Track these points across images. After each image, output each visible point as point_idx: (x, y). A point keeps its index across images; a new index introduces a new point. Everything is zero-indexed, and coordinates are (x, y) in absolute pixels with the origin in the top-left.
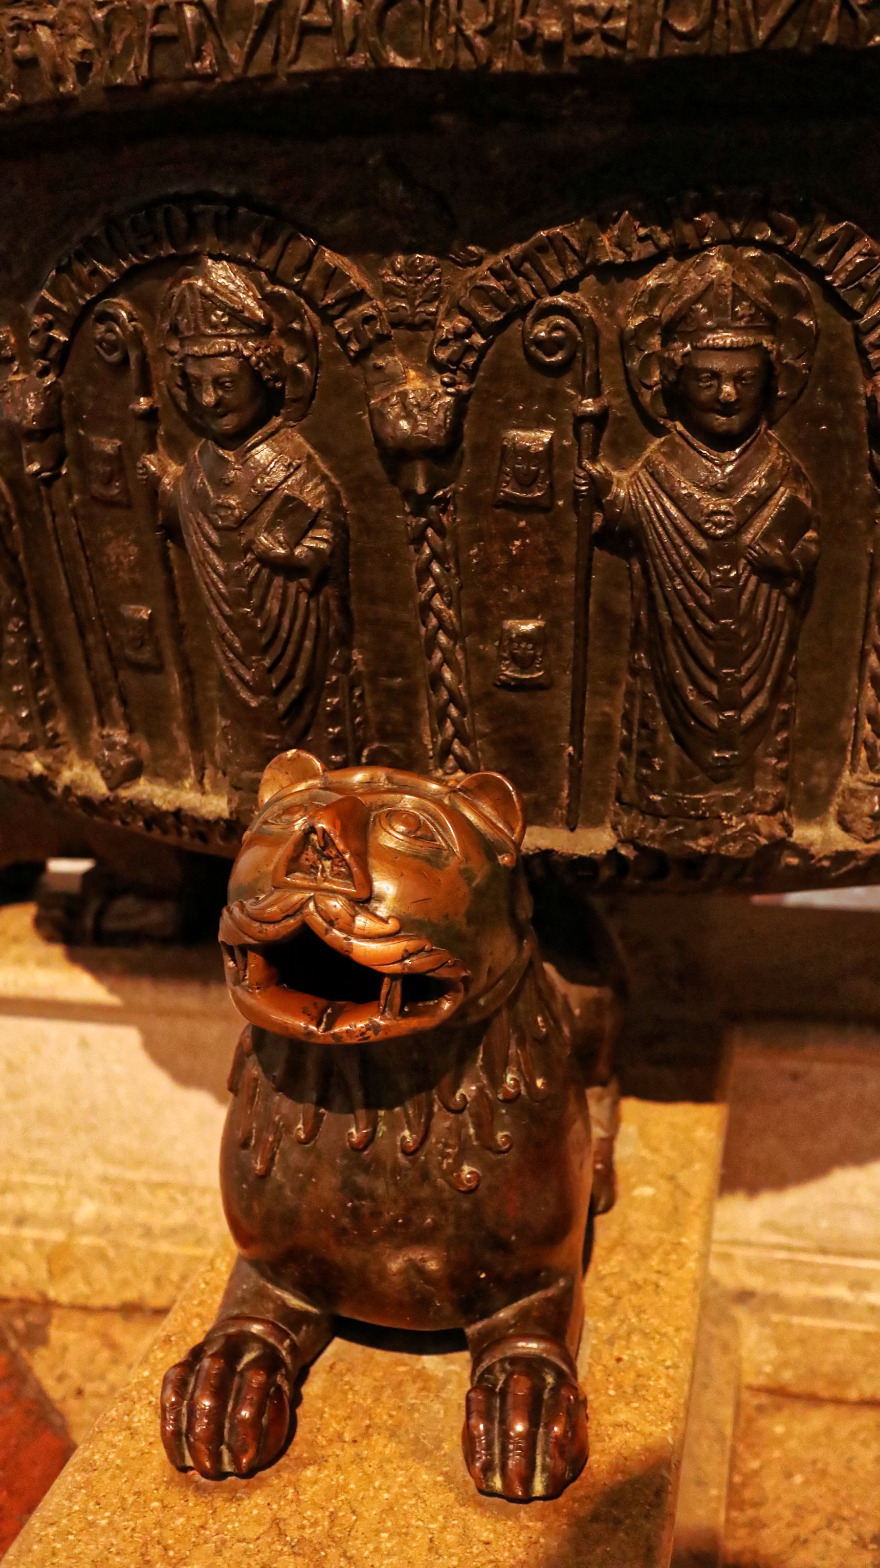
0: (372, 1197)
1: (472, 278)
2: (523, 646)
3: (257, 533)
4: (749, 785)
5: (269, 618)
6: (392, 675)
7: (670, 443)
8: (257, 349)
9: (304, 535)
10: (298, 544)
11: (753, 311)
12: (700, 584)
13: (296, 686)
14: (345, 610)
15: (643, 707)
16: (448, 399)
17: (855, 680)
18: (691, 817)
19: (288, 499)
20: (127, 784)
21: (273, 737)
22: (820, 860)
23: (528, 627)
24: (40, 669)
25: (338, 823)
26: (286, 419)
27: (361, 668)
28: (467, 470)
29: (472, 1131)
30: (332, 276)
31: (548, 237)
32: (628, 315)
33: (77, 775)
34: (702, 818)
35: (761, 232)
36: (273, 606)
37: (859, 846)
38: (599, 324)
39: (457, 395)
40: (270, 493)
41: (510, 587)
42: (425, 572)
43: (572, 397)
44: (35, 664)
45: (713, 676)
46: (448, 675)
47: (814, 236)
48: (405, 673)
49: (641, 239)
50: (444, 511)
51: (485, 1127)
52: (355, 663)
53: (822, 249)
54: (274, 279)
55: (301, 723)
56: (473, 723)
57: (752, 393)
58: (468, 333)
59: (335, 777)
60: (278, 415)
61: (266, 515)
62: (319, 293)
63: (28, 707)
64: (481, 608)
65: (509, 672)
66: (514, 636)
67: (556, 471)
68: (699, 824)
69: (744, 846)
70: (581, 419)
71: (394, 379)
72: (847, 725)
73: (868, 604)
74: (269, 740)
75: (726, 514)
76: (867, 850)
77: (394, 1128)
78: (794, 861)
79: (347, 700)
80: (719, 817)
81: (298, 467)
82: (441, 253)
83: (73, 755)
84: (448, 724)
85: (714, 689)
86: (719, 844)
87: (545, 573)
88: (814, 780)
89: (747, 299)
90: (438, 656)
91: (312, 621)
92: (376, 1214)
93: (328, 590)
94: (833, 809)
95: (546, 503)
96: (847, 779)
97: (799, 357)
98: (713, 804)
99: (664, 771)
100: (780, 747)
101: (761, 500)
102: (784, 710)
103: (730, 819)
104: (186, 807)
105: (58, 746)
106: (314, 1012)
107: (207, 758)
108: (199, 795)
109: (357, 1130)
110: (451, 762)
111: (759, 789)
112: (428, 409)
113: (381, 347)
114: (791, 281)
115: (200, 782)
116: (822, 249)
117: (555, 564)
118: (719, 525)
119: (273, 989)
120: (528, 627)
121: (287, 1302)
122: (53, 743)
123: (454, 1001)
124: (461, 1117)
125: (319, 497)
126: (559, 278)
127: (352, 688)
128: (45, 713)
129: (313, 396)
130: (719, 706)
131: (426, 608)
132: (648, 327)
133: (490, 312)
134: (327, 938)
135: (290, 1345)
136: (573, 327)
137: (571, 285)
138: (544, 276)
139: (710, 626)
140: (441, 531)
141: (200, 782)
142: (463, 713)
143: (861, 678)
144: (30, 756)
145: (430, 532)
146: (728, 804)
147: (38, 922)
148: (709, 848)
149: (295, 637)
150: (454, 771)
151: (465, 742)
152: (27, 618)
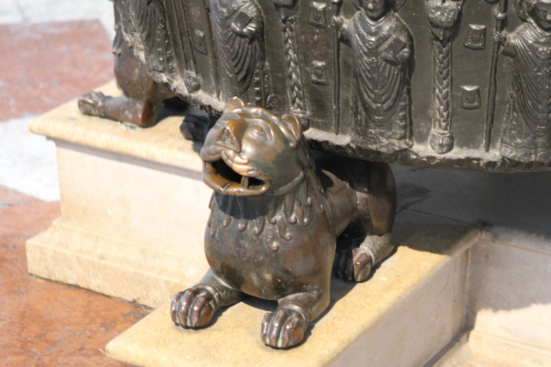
0: (244, 248)
3: (231, 22)
4: (390, 129)
5: (235, 49)
6: (278, 72)
7: (361, 14)
9: (247, 24)
10: (245, 27)
12: (366, 62)
13: (243, 73)
17: (433, 96)
18: (369, 137)
19: (242, 13)
20: (195, 92)
21: (237, 88)
22: (423, 158)
23: (320, 64)
24: (168, 44)
25: (233, 128)
27: (268, 68)
28: (300, 12)
29: (278, 231)
33: (179, 84)
36: (237, 46)
37: (437, 155)
40: (236, 11)
41: (314, 50)
42: (286, 41)
44: (167, 41)
45: (372, 92)
46: (294, 76)
50: (292, 23)
51: (283, 230)
52: (266, 66)
55: (245, 85)
57: (379, 7)
59: (246, 109)
61: (235, 16)
63: (163, 57)
64: (305, 56)
65: (314, 78)
66: (315, 67)
67: (327, 16)
68: (373, 140)
72: (431, 112)
73: (434, 72)
74: (235, 89)
75: (373, 42)
76: (439, 157)
77: (252, 227)
78: (414, 157)
79: (262, 79)
80: (379, 139)
83: (178, 76)
84: (295, 92)
85: (372, 96)
86: (380, 148)
87: (325, 48)
88: (421, 129)
90: (291, 69)
91: (250, 52)
92: (245, 253)
93: (256, 42)
94: (429, 140)
95: (324, 26)
96: (433, 131)
98: (377, 134)
99: (361, 120)
100: (401, 117)
102: (402, 106)
103: (383, 140)
104: (212, 105)
105: (173, 72)
106: (223, 184)
107: (221, 88)
108: (218, 101)
109: (241, 225)
110: (296, 105)
111: (393, 130)
115: (218, 96)
117: (328, 45)
118: (370, 45)
119: (213, 175)
120: (320, 64)
121: (221, 283)
122: (171, 71)
124: (274, 226)
125: (253, 13)
127: (264, 75)
128: (169, 60)
130: (375, 102)
131: (287, 53)
134: (226, 162)
135: (218, 295)
139: (369, 76)
140: (291, 30)
141: (218, 96)
142: (299, 89)
143: (434, 96)
144: (163, 75)
145: (288, 29)
146: (382, 135)
147: (182, 128)
149: (243, 57)
150: (297, 108)
151: (300, 99)
152: (165, 24)
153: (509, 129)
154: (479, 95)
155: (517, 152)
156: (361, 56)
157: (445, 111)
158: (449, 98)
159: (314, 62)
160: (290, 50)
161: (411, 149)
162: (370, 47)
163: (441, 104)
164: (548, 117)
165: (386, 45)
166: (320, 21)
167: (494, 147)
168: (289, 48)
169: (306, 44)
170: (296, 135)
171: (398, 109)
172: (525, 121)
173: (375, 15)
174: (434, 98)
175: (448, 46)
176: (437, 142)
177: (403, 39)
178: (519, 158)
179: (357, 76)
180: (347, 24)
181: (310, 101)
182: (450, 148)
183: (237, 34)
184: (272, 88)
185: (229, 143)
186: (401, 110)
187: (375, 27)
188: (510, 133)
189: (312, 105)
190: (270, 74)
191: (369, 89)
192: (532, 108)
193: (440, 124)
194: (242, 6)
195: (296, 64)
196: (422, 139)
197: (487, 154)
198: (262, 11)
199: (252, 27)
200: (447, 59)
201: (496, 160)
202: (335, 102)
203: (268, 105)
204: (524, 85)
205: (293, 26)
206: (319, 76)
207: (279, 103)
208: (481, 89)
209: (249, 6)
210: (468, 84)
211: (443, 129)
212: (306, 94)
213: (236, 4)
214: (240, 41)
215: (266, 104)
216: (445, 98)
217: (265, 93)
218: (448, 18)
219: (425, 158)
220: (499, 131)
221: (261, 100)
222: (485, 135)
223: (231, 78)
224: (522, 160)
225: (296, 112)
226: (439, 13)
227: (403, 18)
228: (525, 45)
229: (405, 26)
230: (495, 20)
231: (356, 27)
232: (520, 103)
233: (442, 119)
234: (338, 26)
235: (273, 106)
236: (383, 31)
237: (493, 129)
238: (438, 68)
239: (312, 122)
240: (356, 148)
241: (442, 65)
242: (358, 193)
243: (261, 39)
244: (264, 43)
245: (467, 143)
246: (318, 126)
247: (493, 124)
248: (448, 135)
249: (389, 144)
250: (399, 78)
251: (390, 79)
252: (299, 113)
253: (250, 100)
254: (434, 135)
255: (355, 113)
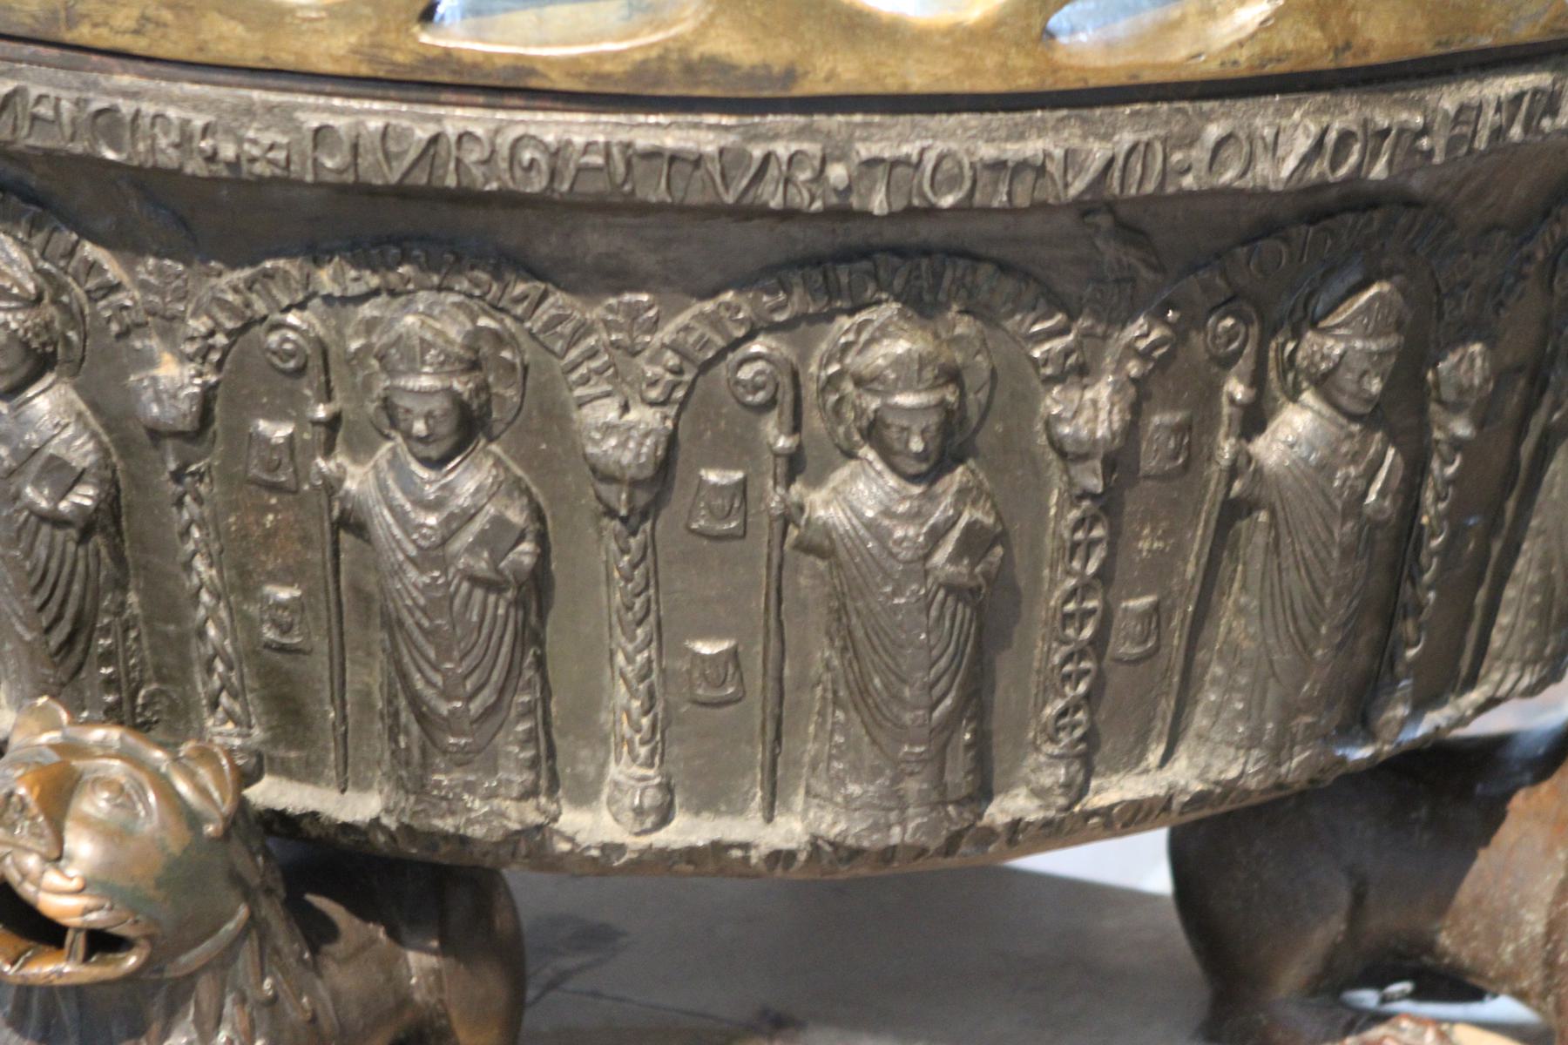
1: (212, 288)
2: (280, 612)
4: (493, 770)
5: (38, 560)
6: (167, 621)
7: (393, 451)
8: (25, 321)
9: (70, 489)
10: (63, 497)
11: (442, 358)
12: (415, 585)
13: (64, 628)
14: (119, 559)
15: (390, 685)
16: (196, 390)
19: (52, 458)
22: (589, 848)
23: (284, 594)
25: (37, 790)
26: (60, 376)
27: (137, 611)
28: (220, 448)
30: (93, 267)
31: (272, 268)
32: (351, 337)
34: (444, 798)
35: (460, 283)
36: (42, 552)
38: (327, 340)
39: (204, 385)
42: (185, 533)
43: (307, 398)
45: (436, 668)
46: (212, 631)
47: (509, 289)
48: (178, 621)
49: (356, 280)
53: (518, 300)
54: (43, 256)
55: (73, 661)
56: (241, 678)
57: (443, 429)
58: (212, 333)
59: (73, 732)
60: (52, 369)
61: (35, 466)
62: (82, 278)
64: (243, 573)
65: (269, 634)
66: (271, 602)
67: (299, 459)
68: (444, 804)
69: (489, 830)
70: (316, 423)
71: (149, 361)
72: (605, 717)
73: (609, 607)
75: (431, 527)
76: (635, 843)
78: (564, 847)
79: (120, 643)
81: (66, 425)
82: (187, 264)
84: (216, 677)
85: (438, 679)
87: (299, 547)
88: (580, 768)
89: (435, 348)
90: (202, 612)
91: (81, 567)
93: (98, 540)
94: (604, 797)
95: (293, 488)
96: (614, 771)
97: (510, 386)
98: (456, 786)
99: (408, 749)
101: (468, 516)
102: (523, 703)
106: (12, 954)
110: (220, 713)
111: (502, 775)
112: (174, 396)
113: (141, 331)
114: (492, 324)
116: (518, 300)
117: (306, 540)
118: (424, 537)
120: (284, 594)
123: (139, 956)
125: (86, 455)
126: (286, 302)
127: (126, 631)
129: (83, 359)
130: (447, 696)
131: (188, 566)
132: (366, 349)
133: (230, 319)
134: (19, 890)
136: (301, 341)
137: (301, 306)
138: (273, 298)
139: (426, 623)
140: (198, 499)
142: (230, 667)
143: (613, 672)
145: (188, 499)
146: (470, 787)
148: (457, 828)
150: (224, 722)
151: (234, 695)
153: (825, 756)
154: (738, 666)
155: (850, 820)
156: (400, 566)
157: (646, 713)
158: (654, 677)
159: (269, 589)
160: (198, 557)
161: (556, 826)
162: (424, 543)
163: (633, 694)
164: (930, 719)
165: (467, 537)
166: (279, 472)
167: (788, 809)
168: (194, 554)
169: (245, 537)
170: (224, 800)
171: (513, 713)
172: (868, 733)
173: (434, 452)
174: (613, 678)
175: (644, 531)
176: (627, 801)
177: (516, 516)
178: (858, 836)
179: (392, 624)
180: (357, 479)
181: (263, 699)
182: (664, 816)
183: (43, 518)
184: (149, 666)
185: (25, 832)
186: (522, 716)
187: (436, 486)
188: (828, 769)
189: (268, 712)
190: (141, 625)
191: (428, 661)
192: (885, 695)
193: (631, 751)
194: (54, 436)
195: (217, 596)
196: (585, 795)
197: (769, 829)
198: (113, 450)
199: (84, 496)
200: (642, 567)
201: (792, 845)
202: (333, 700)
203: (141, 715)
204: (859, 633)
205: (203, 489)
206: (285, 629)
207: (173, 708)
208: (740, 649)
209: (74, 438)
210: (706, 634)
211: (641, 765)
212: (248, 682)
213: (36, 431)
214: (53, 538)
215: (133, 715)
216: (642, 678)
217: (129, 682)
218: (638, 455)
219: (595, 847)
220: (797, 763)
221: (119, 703)
222: (759, 777)
223: (29, 643)
224: (866, 844)
225: (222, 732)
226: (613, 442)
227: (513, 458)
228: (855, 521)
229: (518, 480)
230: (768, 456)
231: (382, 487)
232: (853, 685)
233: (637, 738)
234: (331, 486)
235: (155, 719)
236: (458, 496)
237: (780, 760)
238: (618, 595)
239: (271, 759)
240: (398, 828)
241: (630, 586)
242: (412, 957)
243: (112, 529)
244: (123, 541)
245: (710, 801)
246: (286, 771)
247: (780, 744)
248: (657, 780)
249: (491, 812)
250: (510, 627)
251: (485, 631)
252: (230, 735)
253: (87, 702)
254: (616, 784)
255: (391, 729)
